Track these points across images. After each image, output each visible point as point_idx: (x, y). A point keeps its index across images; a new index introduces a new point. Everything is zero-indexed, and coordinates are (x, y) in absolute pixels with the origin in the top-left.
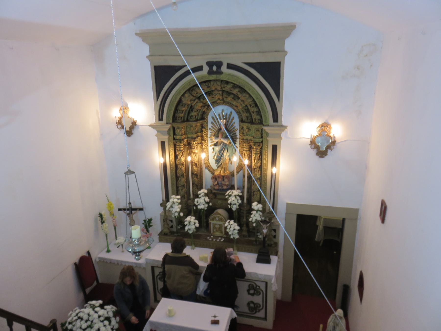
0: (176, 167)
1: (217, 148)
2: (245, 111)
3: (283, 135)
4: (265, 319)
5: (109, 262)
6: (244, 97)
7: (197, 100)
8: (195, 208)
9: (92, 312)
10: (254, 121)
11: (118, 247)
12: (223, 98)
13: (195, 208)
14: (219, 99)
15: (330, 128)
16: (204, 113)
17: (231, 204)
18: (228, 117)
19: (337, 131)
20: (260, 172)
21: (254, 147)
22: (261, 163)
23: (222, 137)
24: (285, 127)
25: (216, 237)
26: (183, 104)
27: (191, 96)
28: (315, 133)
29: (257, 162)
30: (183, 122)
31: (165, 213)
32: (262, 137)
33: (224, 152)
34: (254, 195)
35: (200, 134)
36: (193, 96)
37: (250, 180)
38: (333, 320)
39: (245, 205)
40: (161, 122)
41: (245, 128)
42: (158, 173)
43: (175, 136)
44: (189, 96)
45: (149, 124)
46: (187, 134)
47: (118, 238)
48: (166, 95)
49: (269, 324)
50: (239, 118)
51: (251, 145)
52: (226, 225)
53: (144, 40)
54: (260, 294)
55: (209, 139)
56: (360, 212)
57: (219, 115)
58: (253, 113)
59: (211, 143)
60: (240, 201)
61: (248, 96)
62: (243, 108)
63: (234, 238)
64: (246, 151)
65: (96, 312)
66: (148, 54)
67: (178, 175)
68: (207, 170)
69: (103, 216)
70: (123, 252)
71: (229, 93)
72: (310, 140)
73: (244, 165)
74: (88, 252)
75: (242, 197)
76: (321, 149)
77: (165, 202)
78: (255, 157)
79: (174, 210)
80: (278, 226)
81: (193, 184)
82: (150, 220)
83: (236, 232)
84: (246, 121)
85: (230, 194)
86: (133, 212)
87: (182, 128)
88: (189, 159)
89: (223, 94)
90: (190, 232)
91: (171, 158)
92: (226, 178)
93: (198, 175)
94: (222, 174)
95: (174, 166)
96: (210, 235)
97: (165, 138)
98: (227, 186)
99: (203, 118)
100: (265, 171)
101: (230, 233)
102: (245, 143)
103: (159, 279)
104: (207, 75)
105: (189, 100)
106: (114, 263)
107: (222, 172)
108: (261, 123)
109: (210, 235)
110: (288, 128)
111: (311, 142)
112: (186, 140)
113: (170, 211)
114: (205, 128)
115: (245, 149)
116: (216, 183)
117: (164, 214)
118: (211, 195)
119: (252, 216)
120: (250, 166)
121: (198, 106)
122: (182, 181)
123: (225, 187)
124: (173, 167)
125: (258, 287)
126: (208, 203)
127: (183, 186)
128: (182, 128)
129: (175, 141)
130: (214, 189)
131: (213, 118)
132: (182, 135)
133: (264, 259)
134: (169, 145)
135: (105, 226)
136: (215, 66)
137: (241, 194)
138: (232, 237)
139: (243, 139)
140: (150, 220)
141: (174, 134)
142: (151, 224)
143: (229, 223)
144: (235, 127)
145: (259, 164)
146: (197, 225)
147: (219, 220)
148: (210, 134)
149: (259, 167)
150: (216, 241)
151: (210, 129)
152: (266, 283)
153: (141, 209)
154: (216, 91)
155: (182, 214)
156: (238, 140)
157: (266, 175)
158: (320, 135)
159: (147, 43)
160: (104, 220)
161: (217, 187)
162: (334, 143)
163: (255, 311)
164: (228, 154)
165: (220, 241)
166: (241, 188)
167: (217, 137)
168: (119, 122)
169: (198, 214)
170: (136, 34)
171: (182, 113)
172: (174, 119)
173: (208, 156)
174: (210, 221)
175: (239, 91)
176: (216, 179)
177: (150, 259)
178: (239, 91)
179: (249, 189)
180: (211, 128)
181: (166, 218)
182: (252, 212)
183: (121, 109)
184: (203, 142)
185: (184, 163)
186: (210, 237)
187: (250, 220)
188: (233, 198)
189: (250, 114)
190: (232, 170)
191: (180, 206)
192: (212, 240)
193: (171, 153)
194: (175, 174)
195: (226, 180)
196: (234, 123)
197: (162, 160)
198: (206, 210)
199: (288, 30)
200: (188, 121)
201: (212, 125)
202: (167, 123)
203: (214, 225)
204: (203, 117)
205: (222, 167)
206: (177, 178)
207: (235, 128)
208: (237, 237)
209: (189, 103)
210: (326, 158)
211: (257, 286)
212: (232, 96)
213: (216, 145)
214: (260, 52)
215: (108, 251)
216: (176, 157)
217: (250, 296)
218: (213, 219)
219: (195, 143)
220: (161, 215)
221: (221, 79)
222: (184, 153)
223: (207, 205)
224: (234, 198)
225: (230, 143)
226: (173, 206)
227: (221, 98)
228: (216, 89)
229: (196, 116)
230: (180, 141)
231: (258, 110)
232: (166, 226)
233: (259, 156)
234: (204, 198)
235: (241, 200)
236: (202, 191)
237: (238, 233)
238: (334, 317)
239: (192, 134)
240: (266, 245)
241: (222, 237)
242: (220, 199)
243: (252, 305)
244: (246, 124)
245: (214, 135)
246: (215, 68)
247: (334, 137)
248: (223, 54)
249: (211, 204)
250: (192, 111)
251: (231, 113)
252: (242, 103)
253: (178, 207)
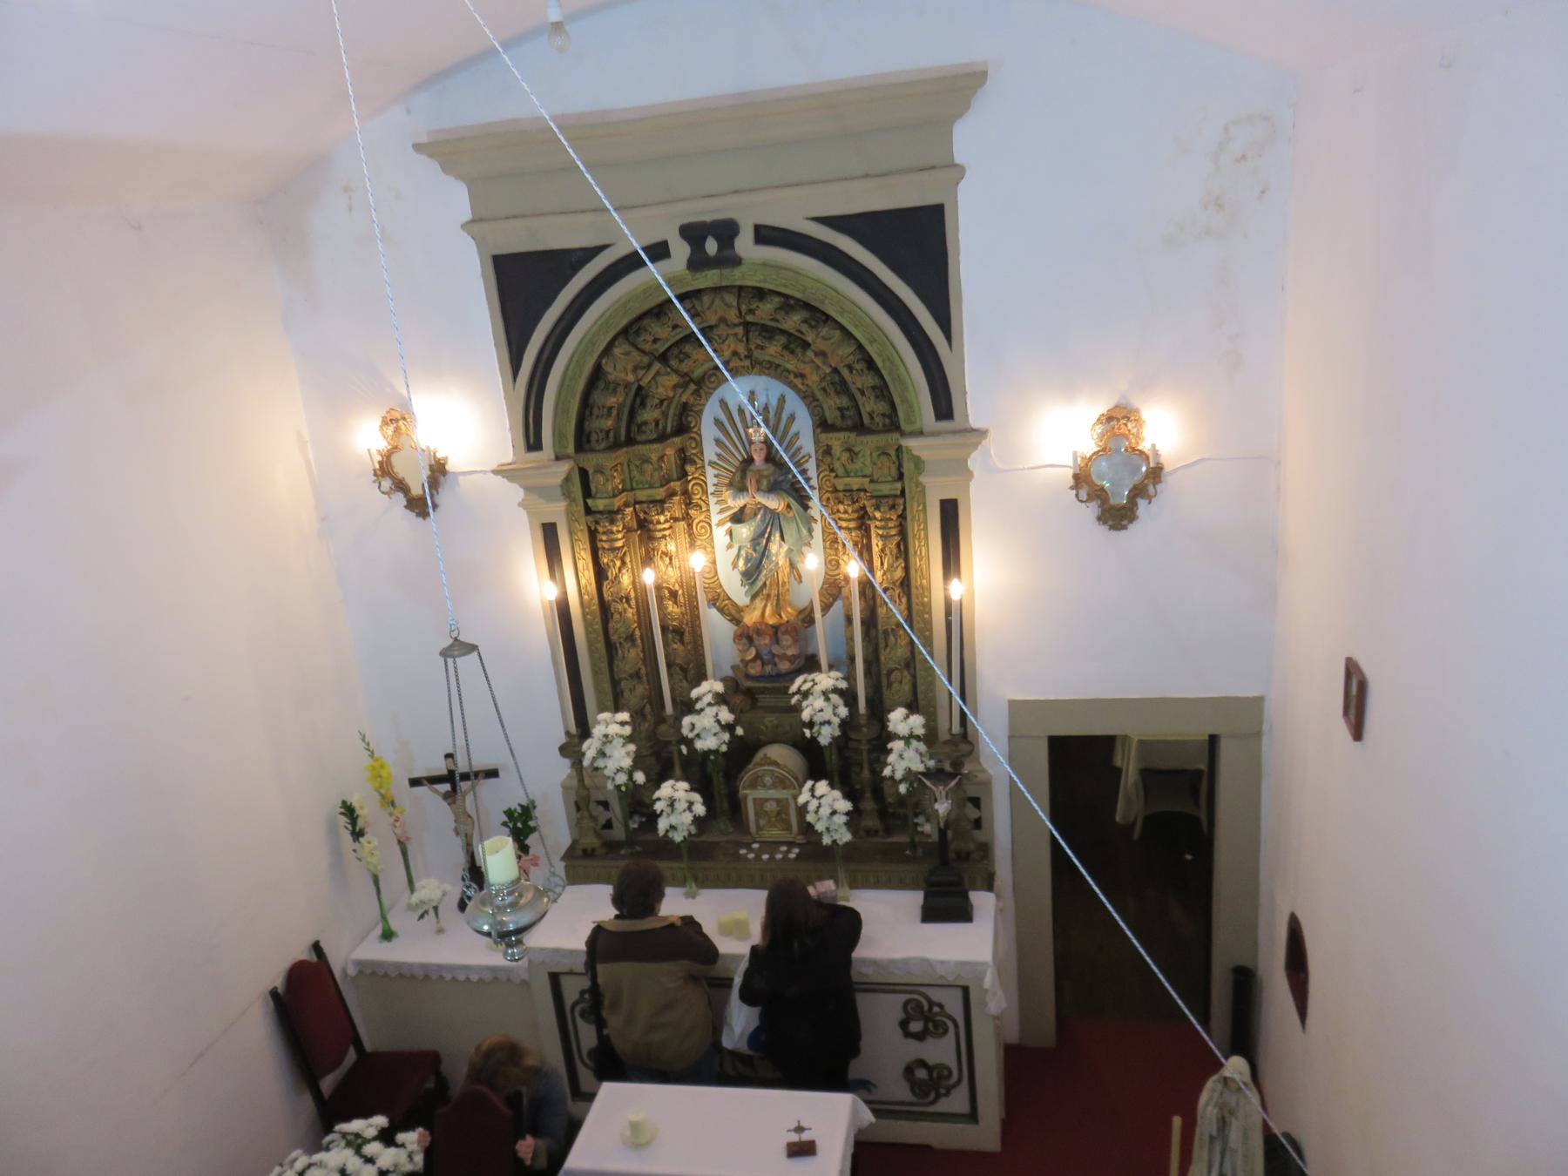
0: (605, 608)
1: (745, 531)
2: (831, 390)
3: (974, 461)
4: (972, 1116)
5: (393, 974)
6: (824, 339)
7: (657, 366)
8: (684, 749)
9: (353, 1162)
10: (866, 420)
11: (422, 916)
12: (749, 350)
13: (684, 749)
14: (735, 353)
15: (1139, 422)
16: (685, 408)
17: (811, 725)
18: (772, 415)
19: (1164, 431)
20: (904, 600)
21: (878, 515)
22: (907, 569)
23: (759, 490)
24: (982, 433)
25: (772, 846)
26: (608, 384)
27: (635, 353)
28: (1088, 445)
29: (891, 566)
30: (615, 446)
31: (581, 780)
32: (901, 477)
33: (768, 540)
34: (890, 685)
35: (678, 486)
36: (643, 352)
37: (873, 633)
38: (1216, 1095)
39: (863, 722)
40: (534, 455)
41: (837, 449)
42: (540, 639)
43: (590, 502)
44: (627, 354)
45: (494, 466)
46: (632, 489)
47: (417, 885)
48: (545, 356)
49: (986, 1135)
50: (812, 415)
51: (863, 508)
52: (802, 799)
53: (447, 168)
54: (946, 1031)
55: (712, 500)
56: (1269, 709)
58: (863, 393)
59: (721, 512)
60: (843, 711)
61: (837, 333)
62: (823, 379)
63: (834, 841)
64: (847, 529)
65: (370, 1160)
66: (467, 215)
67: (614, 638)
68: (714, 611)
69: (358, 812)
70: (440, 931)
71: (769, 332)
72: (1070, 472)
73: (847, 579)
74: (317, 947)
75: (849, 696)
76: (1114, 501)
77: (576, 740)
78: (883, 550)
79: (610, 766)
80: (987, 784)
81: (669, 665)
82: (527, 812)
83: (841, 819)
84: (839, 423)
85: (805, 687)
86: (464, 785)
87: (614, 468)
88: (648, 577)
89: (747, 333)
90: (678, 837)
91: (583, 582)
92: (784, 633)
93: (685, 633)
94: (771, 622)
95: (595, 607)
96: (747, 839)
97: (556, 510)
98: (791, 659)
99: (682, 428)
100: (923, 596)
101: (820, 827)
102: (841, 502)
103: (582, 1015)
104: (688, 275)
105: (630, 367)
106: (413, 977)
107: (769, 609)
108: (893, 425)
109: (747, 839)
110: (991, 435)
111: (1076, 477)
112: (629, 510)
113: (597, 769)
114: (693, 462)
115: (844, 524)
116: (753, 652)
117: (575, 782)
118: (738, 700)
119: (891, 758)
120: (866, 587)
121: (665, 385)
122: (631, 657)
123: (784, 666)
124: (592, 613)
125: (936, 1009)
126: (729, 728)
127: (636, 675)
128: (614, 468)
129: (590, 518)
130: (748, 676)
131: (718, 423)
132: (615, 496)
133: (946, 905)
134: (571, 533)
135: (367, 847)
136: (710, 239)
137: (843, 685)
138: (826, 840)
139: (836, 490)
140: (527, 812)
141: (587, 492)
142: (532, 823)
143: (812, 790)
144: (799, 449)
145: (899, 574)
146: (700, 809)
147: (774, 786)
148: (715, 481)
149: (902, 584)
150: (772, 859)
151: (712, 464)
152: (966, 990)
153: (492, 774)
154: (722, 326)
155: (640, 777)
156: (815, 496)
157: (927, 607)
158: (1103, 451)
159: (458, 177)
160: (360, 824)
161: (755, 670)
162: (1156, 473)
163: (932, 1096)
164: (785, 547)
165: (785, 858)
166: (844, 663)
167: (742, 489)
168: (385, 469)
169: (699, 771)
170: (418, 147)
171: (609, 414)
172: (583, 441)
173: (714, 562)
174: (742, 792)
175: (805, 321)
176: (750, 640)
177: (542, 950)
178: (805, 321)
179: (872, 663)
180: (715, 459)
181: (585, 797)
182: (890, 746)
183: (385, 422)
184: (692, 512)
185: (632, 595)
186: (748, 846)
187: (887, 772)
188: (819, 702)
189: (852, 398)
190: (803, 603)
191: (632, 747)
192: (758, 858)
193: (580, 564)
194: (601, 638)
195: (786, 640)
196: (797, 434)
197: (551, 592)
198: (724, 754)
199: (958, 89)
200: (630, 441)
202: (558, 458)
203: (759, 803)
204: (684, 424)
205: (769, 596)
206: (610, 647)
207: (803, 452)
208: (845, 837)
209: (631, 378)
210: (1133, 527)
211: (931, 1004)
212: (783, 339)
213: (738, 518)
214: (866, 176)
215: (388, 935)
216: (600, 573)
217: (912, 1043)
218: (754, 784)
219: (662, 518)
220: (565, 788)
221: (739, 283)
222: (628, 559)
223: (726, 737)
224: (820, 702)
225: (789, 506)
226: (608, 751)
227: (742, 349)
228: (723, 320)
229: (657, 423)
230: (612, 515)
231: (877, 381)
232: (587, 823)
233: (898, 545)
234: (715, 709)
235: (846, 705)
236: (705, 686)
237: (848, 824)
238: (1219, 1087)
239: (651, 487)
240: (952, 855)
241: (791, 844)
242: (773, 710)
243: (921, 1074)
244: (841, 435)
245: (730, 485)
246: (711, 246)
247: (1156, 453)
248: (736, 192)
249: (740, 731)
250: (643, 404)
251: (782, 400)
252: (818, 361)
253: (623, 751)
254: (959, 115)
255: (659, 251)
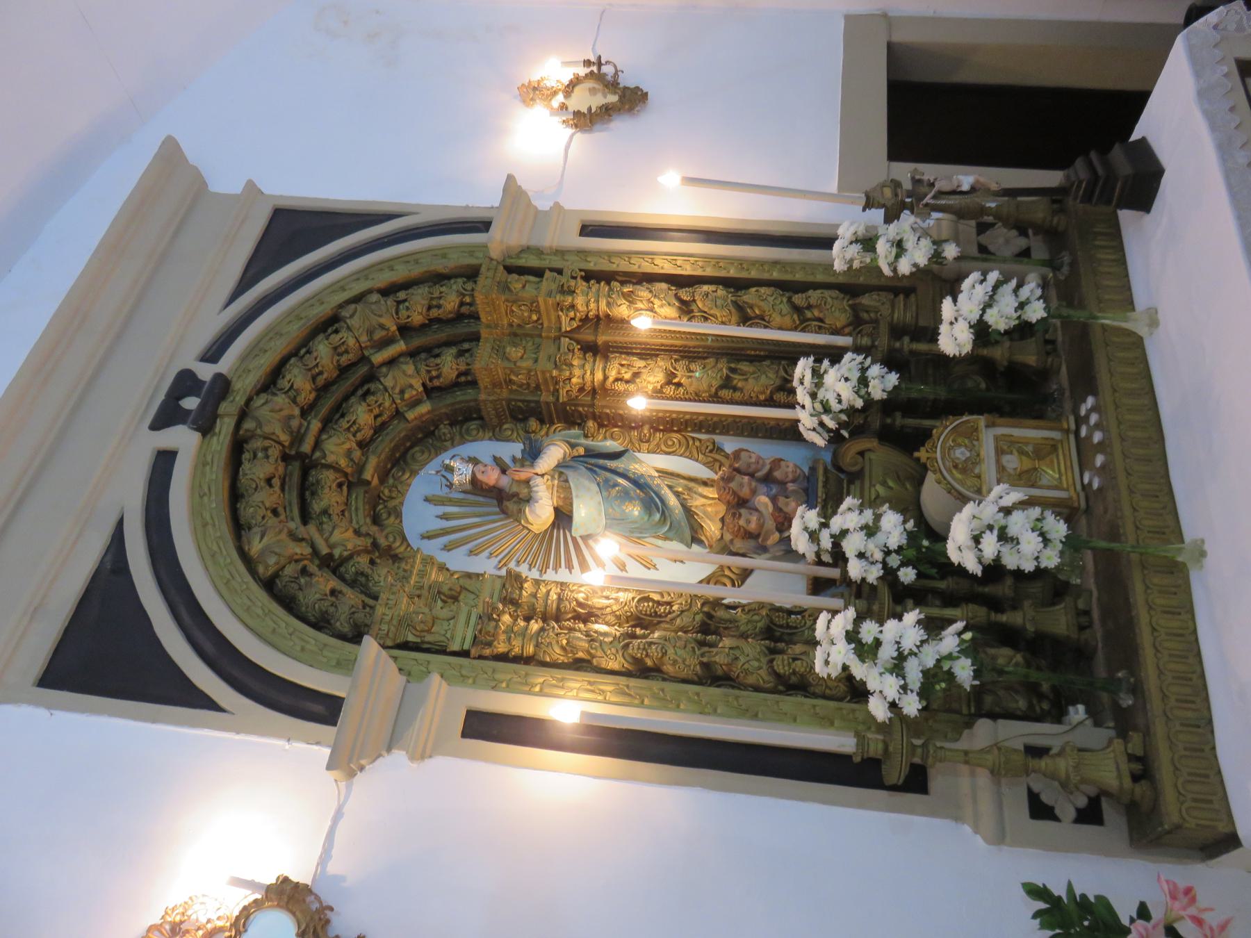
0: (642, 670)
3: (543, 205)
19: (556, 69)
24: (510, 178)
25: (1083, 447)
32: (539, 273)
48: (209, 648)
57: (444, 517)
59: (570, 567)
97: (446, 697)
105: (284, 536)
131: (447, 548)
180: (495, 561)
201: (486, 553)
206: (712, 677)
209: (303, 550)
216: (580, 665)
226: (887, 653)
254: (205, 184)
255: (164, 461)
